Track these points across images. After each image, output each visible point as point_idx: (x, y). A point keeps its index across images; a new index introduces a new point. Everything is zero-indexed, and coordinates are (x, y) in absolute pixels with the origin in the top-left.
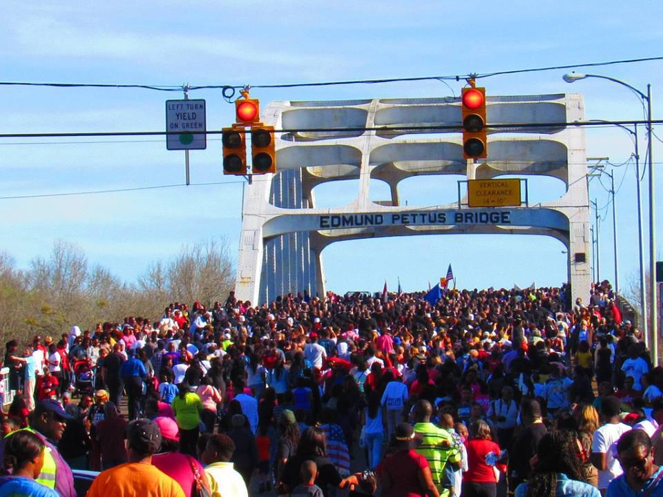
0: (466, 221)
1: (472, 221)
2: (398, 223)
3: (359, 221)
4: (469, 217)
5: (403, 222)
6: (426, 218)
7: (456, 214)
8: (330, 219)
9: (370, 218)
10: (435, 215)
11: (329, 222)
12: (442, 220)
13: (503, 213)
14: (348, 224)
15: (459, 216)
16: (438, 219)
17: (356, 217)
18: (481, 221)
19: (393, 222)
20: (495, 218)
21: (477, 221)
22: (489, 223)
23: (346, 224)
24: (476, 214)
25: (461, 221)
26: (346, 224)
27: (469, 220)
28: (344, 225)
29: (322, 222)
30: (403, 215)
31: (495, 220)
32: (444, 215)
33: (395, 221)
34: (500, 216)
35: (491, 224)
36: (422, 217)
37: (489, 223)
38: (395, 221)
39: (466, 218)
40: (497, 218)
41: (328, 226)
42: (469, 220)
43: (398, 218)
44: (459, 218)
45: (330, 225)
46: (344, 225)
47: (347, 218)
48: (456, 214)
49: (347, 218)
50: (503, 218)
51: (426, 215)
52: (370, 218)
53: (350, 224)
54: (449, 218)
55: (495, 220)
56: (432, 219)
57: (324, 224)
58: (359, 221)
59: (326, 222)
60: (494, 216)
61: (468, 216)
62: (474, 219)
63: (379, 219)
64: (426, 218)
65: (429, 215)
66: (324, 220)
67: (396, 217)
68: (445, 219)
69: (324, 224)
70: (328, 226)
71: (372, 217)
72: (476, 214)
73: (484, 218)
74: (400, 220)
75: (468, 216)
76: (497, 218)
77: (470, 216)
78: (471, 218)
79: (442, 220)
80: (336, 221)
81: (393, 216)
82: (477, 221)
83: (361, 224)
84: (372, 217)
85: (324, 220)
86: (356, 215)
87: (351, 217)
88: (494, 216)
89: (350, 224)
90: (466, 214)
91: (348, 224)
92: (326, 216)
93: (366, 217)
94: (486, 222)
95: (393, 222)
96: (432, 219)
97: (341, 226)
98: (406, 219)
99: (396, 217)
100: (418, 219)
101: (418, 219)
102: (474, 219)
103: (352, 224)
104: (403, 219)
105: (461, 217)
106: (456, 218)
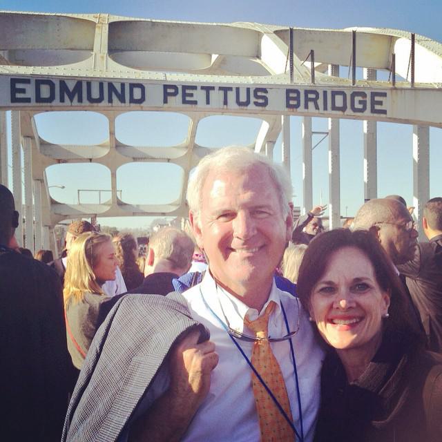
0: (306, 107)
1: (317, 108)
2: (176, 101)
3: (95, 95)
5: (184, 102)
6: (232, 96)
7: (288, 91)
8: (33, 82)
9: (119, 89)
10: (248, 90)
11: (30, 92)
12: (261, 101)
13: (374, 95)
14: (71, 100)
15: (292, 95)
16: (253, 99)
17: (89, 84)
18: (334, 108)
19: (165, 101)
20: (360, 102)
21: (325, 108)
22: (349, 111)
23: (66, 97)
24: (325, 93)
25: (297, 106)
26: (66, 97)
27: (311, 104)
28: (62, 100)
29: (14, 91)
30: (185, 88)
31: (360, 107)
34: (368, 99)
35: (352, 113)
36: (222, 93)
37: (349, 111)
38: (169, 98)
39: (307, 100)
40: (363, 103)
41: (28, 100)
42: (311, 104)
43: (175, 94)
44: (294, 99)
45: (33, 98)
46: (62, 100)
47: (71, 86)
48: (288, 91)
49: (71, 86)
50: (374, 103)
51: (230, 89)
52: (118, 88)
53: (76, 98)
55: (360, 107)
56: (243, 98)
58: (95, 95)
59: (23, 91)
60: (357, 99)
61: (311, 96)
62: (320, 102)
63: (137, 93)
64: (232, 96)
65: (238, 89)
66: (19, 86)
67: (170, 91)
68: (265, 98)
69: (19, 95)
70: (28, 100)
71: (123, 85)
72: (325, 93)
73: (339, 101)
75: (312, 96)
76: (363, 103)
77: (312, 96)
78: (315, 101)
79: (261, 101)
80: (45, 91)
81: (166, 87)
82: (325, 108)
83: (100, 100)
84: (123, 85)
85: (19, 86)
87: (79, 84)
88: (357, 99)
89: (76, 98)
90: (307, 92)
91: (71, 100)
93: (111, 86)
94: (343, 109)
95: (165, 101)
96: (243, 98)
97: (57, 102)
98: (191, 95)
99: (172, 91)
100: (216, 96)
101: (216, 96)
102: (320, 102)
103: (80, 100)
104: (184, 95)
105: (298, 99)
106: (288, 99)
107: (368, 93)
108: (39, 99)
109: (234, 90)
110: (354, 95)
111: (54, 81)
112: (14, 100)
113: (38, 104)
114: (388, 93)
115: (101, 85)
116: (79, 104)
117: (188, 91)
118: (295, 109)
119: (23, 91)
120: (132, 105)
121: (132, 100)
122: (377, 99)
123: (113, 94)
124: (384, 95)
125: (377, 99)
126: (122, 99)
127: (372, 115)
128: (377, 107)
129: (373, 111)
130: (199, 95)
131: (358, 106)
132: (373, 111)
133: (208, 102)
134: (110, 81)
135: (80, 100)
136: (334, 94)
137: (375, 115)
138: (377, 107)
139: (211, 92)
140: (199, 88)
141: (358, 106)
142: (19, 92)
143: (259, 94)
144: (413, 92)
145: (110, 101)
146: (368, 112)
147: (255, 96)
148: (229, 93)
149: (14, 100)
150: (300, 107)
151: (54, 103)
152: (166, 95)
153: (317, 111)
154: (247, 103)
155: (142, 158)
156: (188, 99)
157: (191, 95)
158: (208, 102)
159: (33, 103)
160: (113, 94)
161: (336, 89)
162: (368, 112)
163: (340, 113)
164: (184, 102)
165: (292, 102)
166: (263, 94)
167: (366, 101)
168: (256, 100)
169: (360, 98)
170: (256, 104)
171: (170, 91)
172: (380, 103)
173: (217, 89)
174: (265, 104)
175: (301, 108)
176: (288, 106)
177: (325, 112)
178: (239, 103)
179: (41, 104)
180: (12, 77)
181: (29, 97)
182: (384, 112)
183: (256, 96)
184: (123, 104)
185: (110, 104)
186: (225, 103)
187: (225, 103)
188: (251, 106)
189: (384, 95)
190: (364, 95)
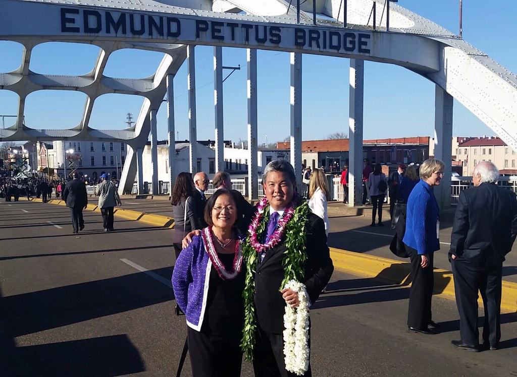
0: (310, 45)
1: (318, 46)
3: (138, 27)
4: (314, 39)
5: (214, 37)
6: (252, 32)
10: (265, 27)
11: (79, 22)
12: (275, 39)
13: (361, 36)
14: (116, 32)
16: (269, 37)
17: (132, 16)
19: (198, 36)
20: (351, 42)
21: (325, 47)
22: (342, 50)
24: (325, 33)
25: (304, 44)
27: (314, 43)
28: (108, 31)
29: (64, 20)
32: (280, 31)
33: (202, 34)
34: (357, 40)
36: (244, 29)
37: (342, 50)
39: (311, 39)
40: (352, 42)
41: (77, 30)
42: (314, 43)
43: (205, 29)
44: (300, 37)
46: (108, 31)
47: (116, 17)
49: (116, 17)
50: (361, 43)
51: (251, 26)
52: (157, 20)
54: (288, 37)
56: (261, 36)
57: (68, 25)
58: (138, 27)
59: (72, 21)
60: (349, 39)
61: (314, 35)
62: (321, 41)
63: (174, 27)
64: (252, 32)
66: (68, 16)
67: (201, 26)
68: (279, 36)
69: (68, 25)
70: (77, 30)
71: (161, 19)
72: (325, 33)
73: (335, 39)
74: (209, 32)
75: (314, 35)
76: (352, 42)
78: (317, 39)
79: (275, 39)
80: (92, 21)
85: (68, 16)
86: (132, 14)
88: (349, 39)
90: (311, 32)
91: (116, 32)
92: (74, 10)
93: (151, 19)
95: (198, 36)
96: (261, 36)
97: (103, 33)
98: (219, 31)
100: (239, 32)
101: (239, 32)
102: (321, 41)
103: (124, 32)
104: (214, 31)
105: (304, 37)
106: (297, 37)
107: (356, 34)
108: (87, 30)
109: (254, 27)
110: (347, 35)
111: (100, 12)
112: (64, 29)
113: (87, 34)
114: (371, 34)
115: (142, 17)
116: (123, 35)
117: (216, 27)
118: (301, 47)
119: (72, 21)
120: (170, 38)
121: (170, 34)
122: (363, 40)
123: (159, 26)
124: (368, 36)
125: (363, 40)
126: (161, 33)
127: (359, 54)
128: (363, 47)
129: (360, 50)
130: (226, 31)
131: (349, 45)
132: (360, 50)
133: (233, 39)
134: (151, 14)
135: (124, 32)
136: (332, 34)
137: (362, 54)
138: (363, 47)
139: (236, 29)
140: (225, 25)
141: (349, 45)
142: (69, 22)
143: (274, 32)
144: (389, 35)
145: (151, 33)
146: (356, 52)
147: (270, 34)
148: (250, 30)
149: (64, 29)
150: (305, 45)
151: (100, 34)
152: (198, 30)
153: (318, 49)
154: (264, 40)
155: (51, 86)
156: (216, 34)
157: (219, 31)
158: (233, 39)
159: (82, 33)
160: (159, 26)
161: (333, 30)
162: (356, 52)
163: (335, 51)
164: (214, 37)
165: (299, 41)
166: (277, 33)
167: (355, 41)
168: (271, 38)
169: (351, 39)
170: (272, 41)
171: (201, 26)
172: (365, 44)
173: (240, 26)
174: (278, 42)
175: (306, 47)
176: (297, 44)
177: (325, 50)
178: (257, 39)
179: (89, 34)
180: (63, 7)
181: (78, 27)
182: (368, 51)
183: (272, 34)
184: (162, 37)
185: (150, 37)
186: (247, 39)
187: (247, 39)
188: (268, 43)
189: (368, 36)
190: (353, 36)
